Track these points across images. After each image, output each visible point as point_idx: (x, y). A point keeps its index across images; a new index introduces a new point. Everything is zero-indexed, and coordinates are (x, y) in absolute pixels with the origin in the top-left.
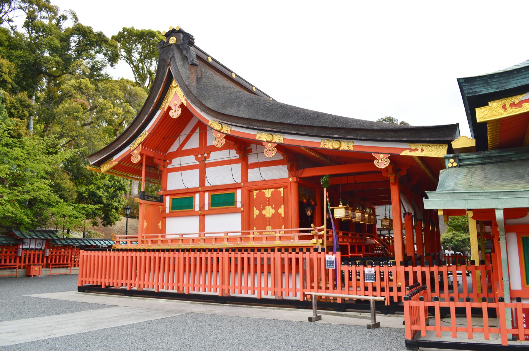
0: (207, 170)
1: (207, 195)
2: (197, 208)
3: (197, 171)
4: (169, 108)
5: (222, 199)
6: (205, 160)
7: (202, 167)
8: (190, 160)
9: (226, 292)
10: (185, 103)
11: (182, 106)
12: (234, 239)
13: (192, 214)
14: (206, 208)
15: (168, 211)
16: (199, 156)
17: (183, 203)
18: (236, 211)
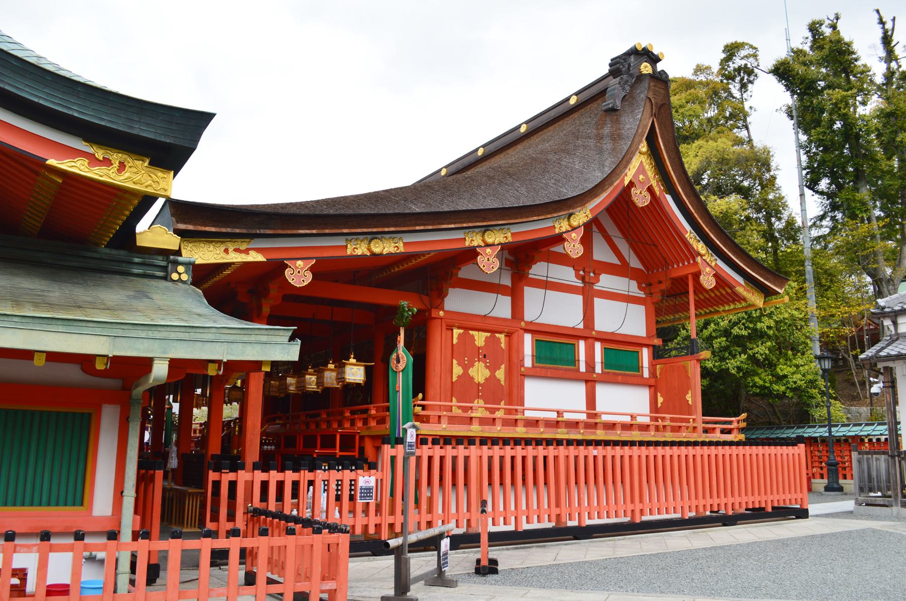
0: (597, 301)
1: (598, 346)
2: (583, 368)
3: (580, 298)
4: (631, 184)
5: (620, 361)
6: (593, 284)
7: (588, 294)
8: (566, 274)
9: (372, 530)
10: (657, 190)
11: (650, 190)
12: (575, 425)
13: (573, 376)
14: (598, 369)
15: (528, 363)
16: (581, 273)
17: (557, 352)
18: (638, 382)
